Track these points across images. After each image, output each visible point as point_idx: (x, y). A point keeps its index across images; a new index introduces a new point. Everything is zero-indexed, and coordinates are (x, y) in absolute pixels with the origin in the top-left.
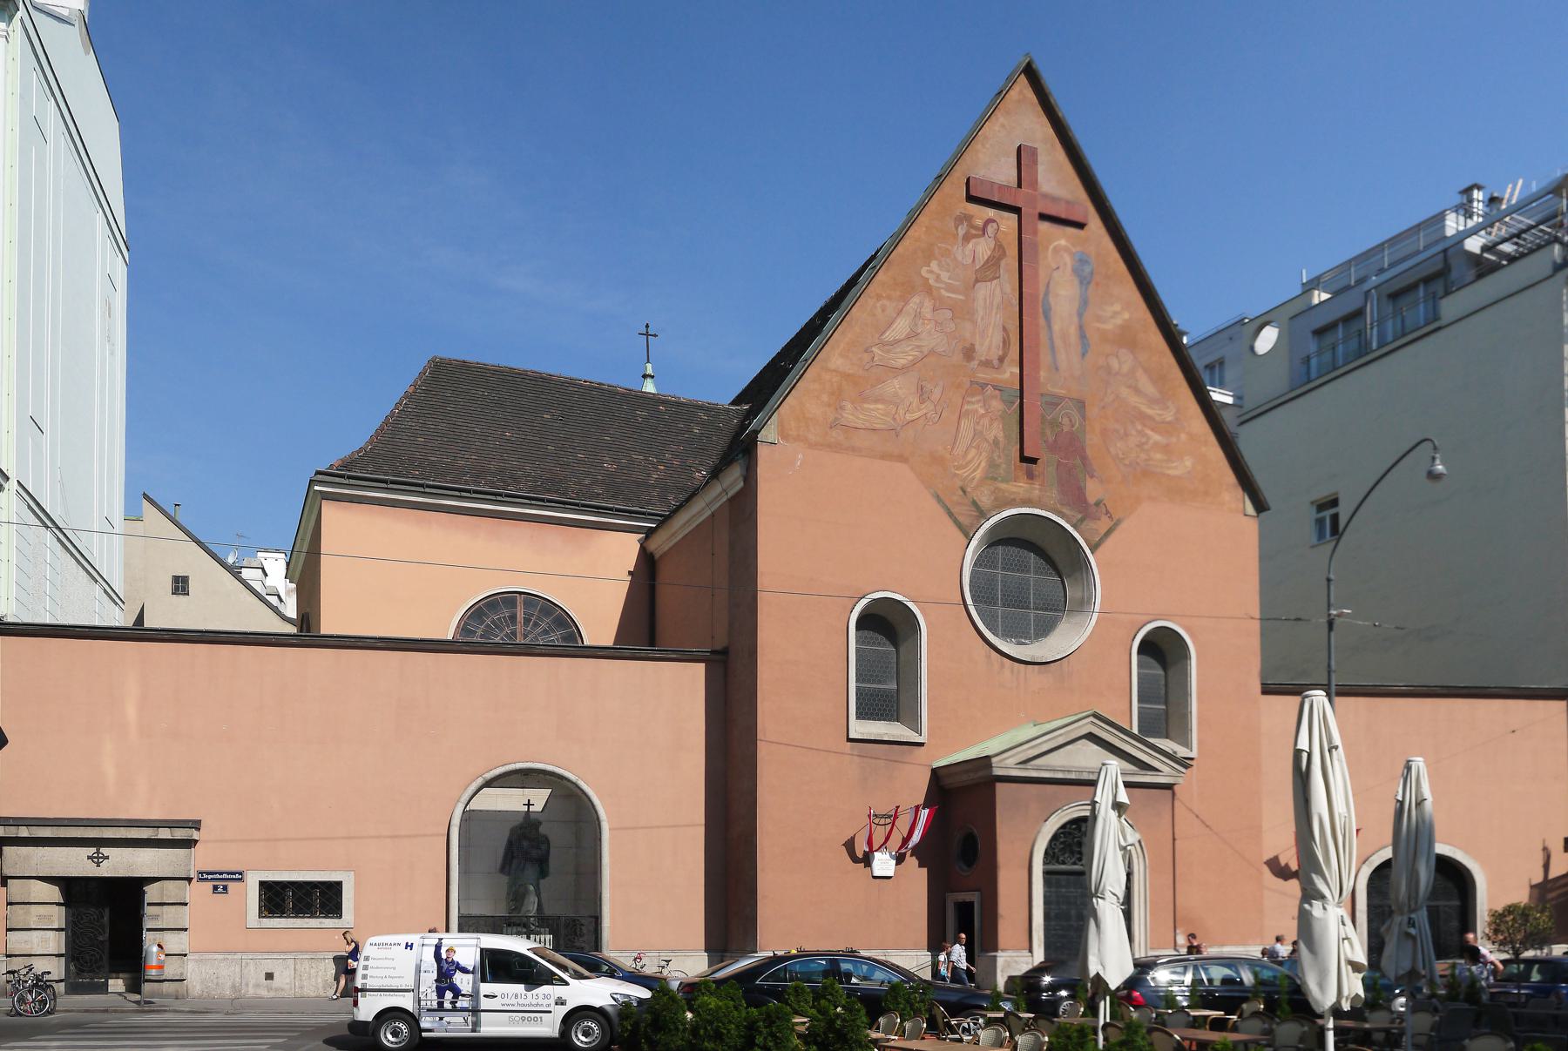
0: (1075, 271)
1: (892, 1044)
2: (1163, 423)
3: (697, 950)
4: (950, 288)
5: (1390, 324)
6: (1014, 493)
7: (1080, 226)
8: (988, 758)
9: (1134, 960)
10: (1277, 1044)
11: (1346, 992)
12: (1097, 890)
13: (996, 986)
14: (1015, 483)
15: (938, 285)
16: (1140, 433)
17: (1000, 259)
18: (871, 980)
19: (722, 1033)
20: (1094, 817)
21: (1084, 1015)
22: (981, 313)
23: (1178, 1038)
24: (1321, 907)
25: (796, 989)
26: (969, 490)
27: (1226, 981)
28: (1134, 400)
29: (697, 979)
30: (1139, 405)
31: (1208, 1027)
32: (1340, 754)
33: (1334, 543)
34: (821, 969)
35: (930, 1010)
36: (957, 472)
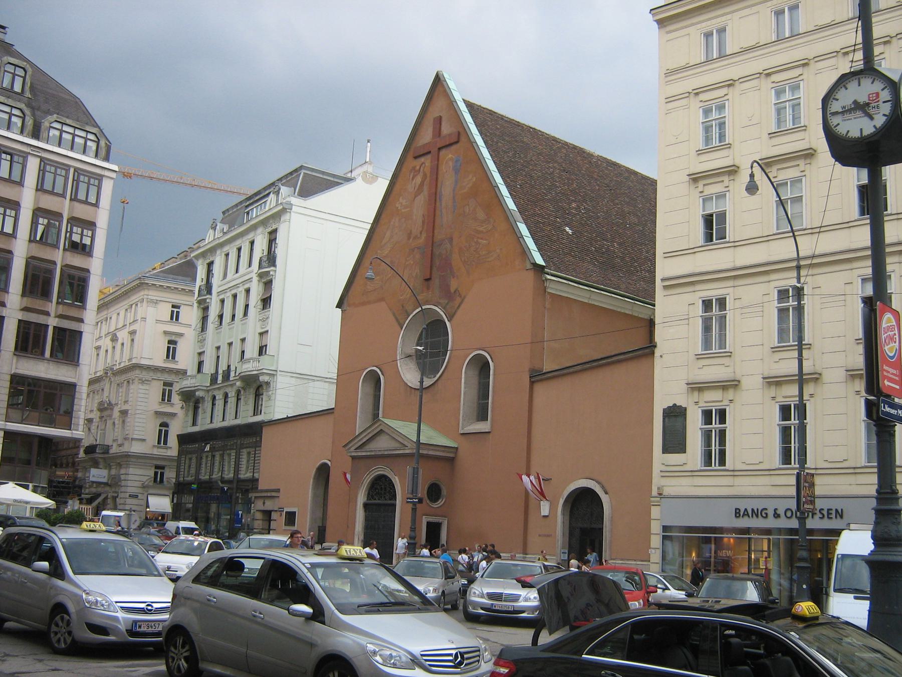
16: (477, 243)
26: (404, 305)
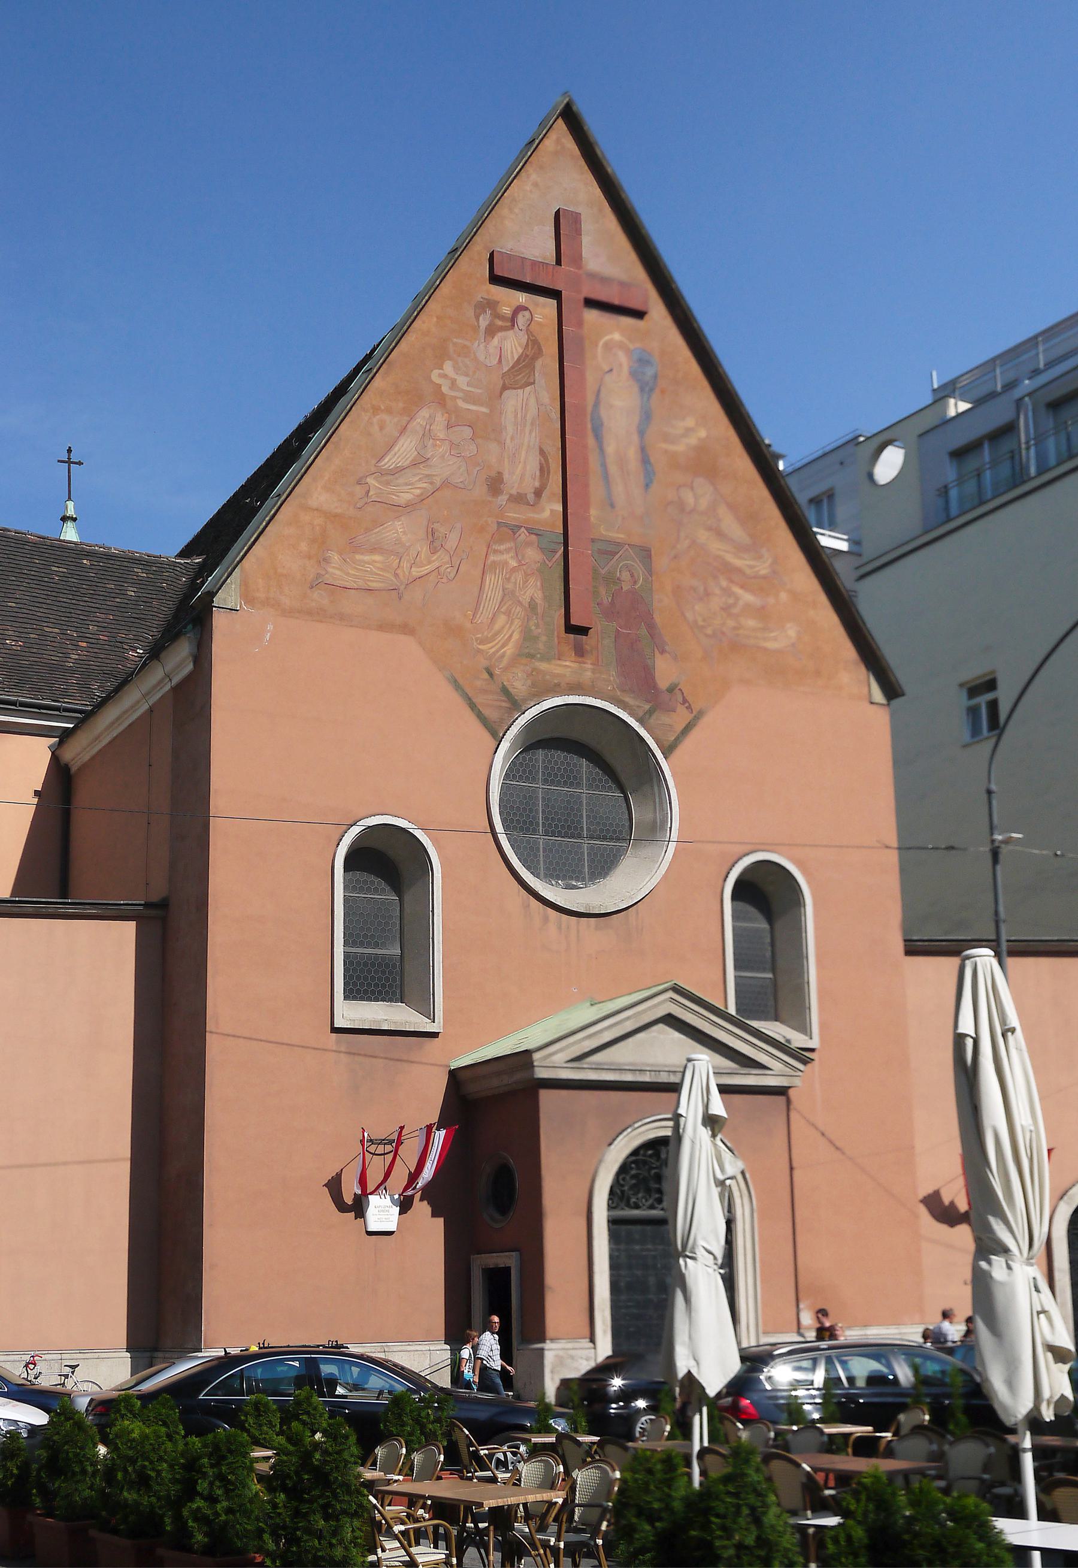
0: (634, 374)
1: (394, 1487)
2: (755, 577)
3: (115, 1349)
4: (469, 398)
5: (1051, 444)
6: (558, 675)
7: (639, 314)
8: (528, 1053)
9: (741, 1350)
10: (952, 1474)
11: (1046, 1393)
12: (685, 1245)
13: (544, 1394)
14: (559, 662)
15: (453, 394)
16: (727, 592)
17: (534, 358)
18: (364, 1389)
19: (149, 1477)
20: (678, 1137)
21: (671, 1436)
22: (510, 429)
23: (808, 1469)
24: (1004, 1265)
25: (257, 1405)
26: (497, 672)
27: (875, 1380)
28: (716, 547)
29: (115, 1394)
30: (721, 553)
31: (850, 1450)
32: (1018, 1039)
33: (993, 740)
34: (293, 1374)
35: (448, 1435)
36: (481, 647)
